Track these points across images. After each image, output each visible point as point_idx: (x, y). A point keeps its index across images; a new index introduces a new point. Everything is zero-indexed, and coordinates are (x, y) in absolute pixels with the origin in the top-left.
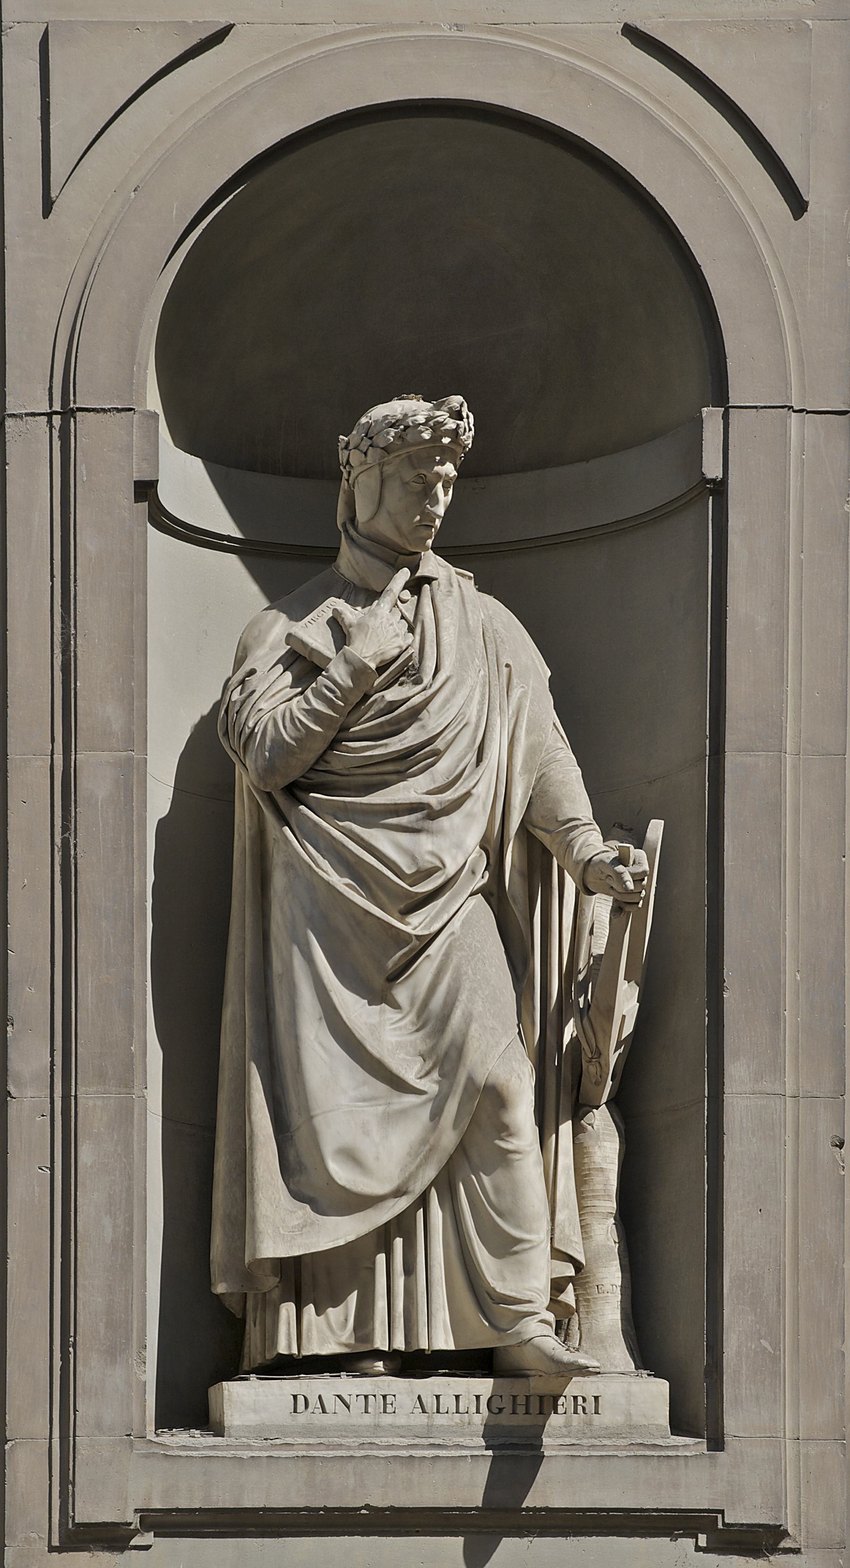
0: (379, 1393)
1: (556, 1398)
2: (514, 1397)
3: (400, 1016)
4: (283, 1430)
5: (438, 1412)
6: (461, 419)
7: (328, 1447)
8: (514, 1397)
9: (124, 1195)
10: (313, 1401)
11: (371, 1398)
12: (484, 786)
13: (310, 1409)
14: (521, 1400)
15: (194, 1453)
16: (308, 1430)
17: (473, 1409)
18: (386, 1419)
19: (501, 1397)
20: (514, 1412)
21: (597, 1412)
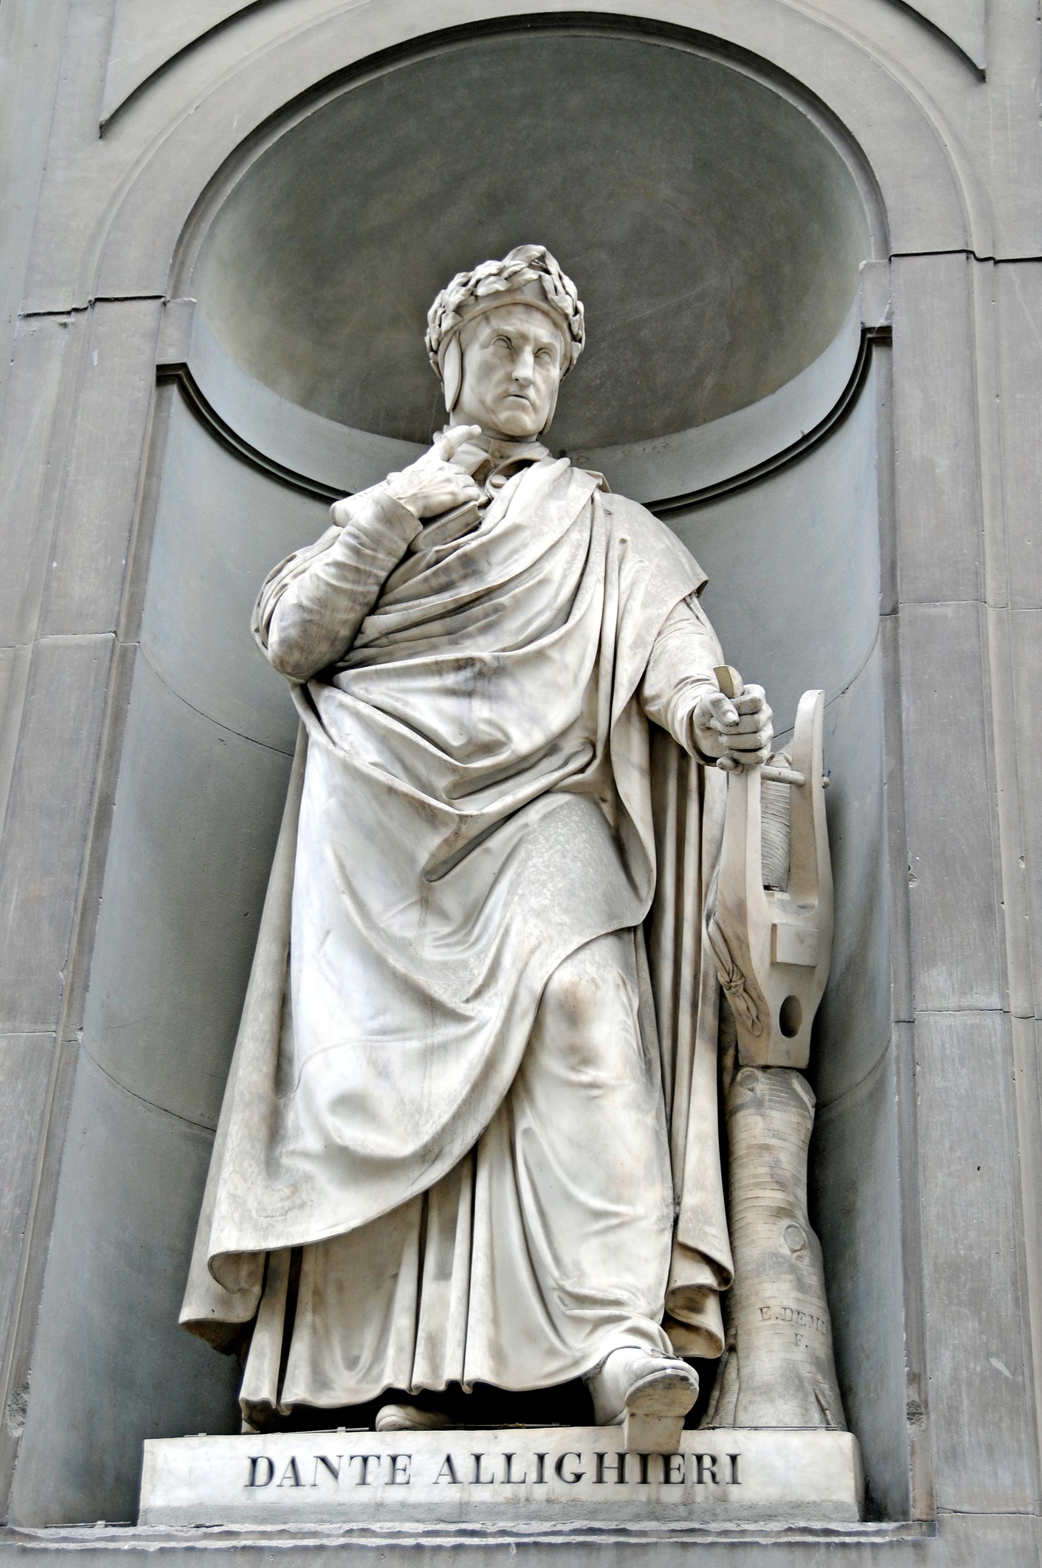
0: (386, 1452)
1: (667, 1459)
2: (601, 1457)
3: (447, 930)
4: (229, 1512)
5: (478, 1481)
6: (547, 272)
7: (294, 1535)
8: (601, 1457)
9: (19, 1164)
10: (282, 1467)
11: (372, 1462)
12: (575, 660)
13: (277, 1479)
14: (611, 1461)
15: (72, 1546)
16: (270, 1513)
17: (533, 1476)
18: (395, 1495)
19: (579, 1456)
20: (600, 1480)
21: (735, 1481)
